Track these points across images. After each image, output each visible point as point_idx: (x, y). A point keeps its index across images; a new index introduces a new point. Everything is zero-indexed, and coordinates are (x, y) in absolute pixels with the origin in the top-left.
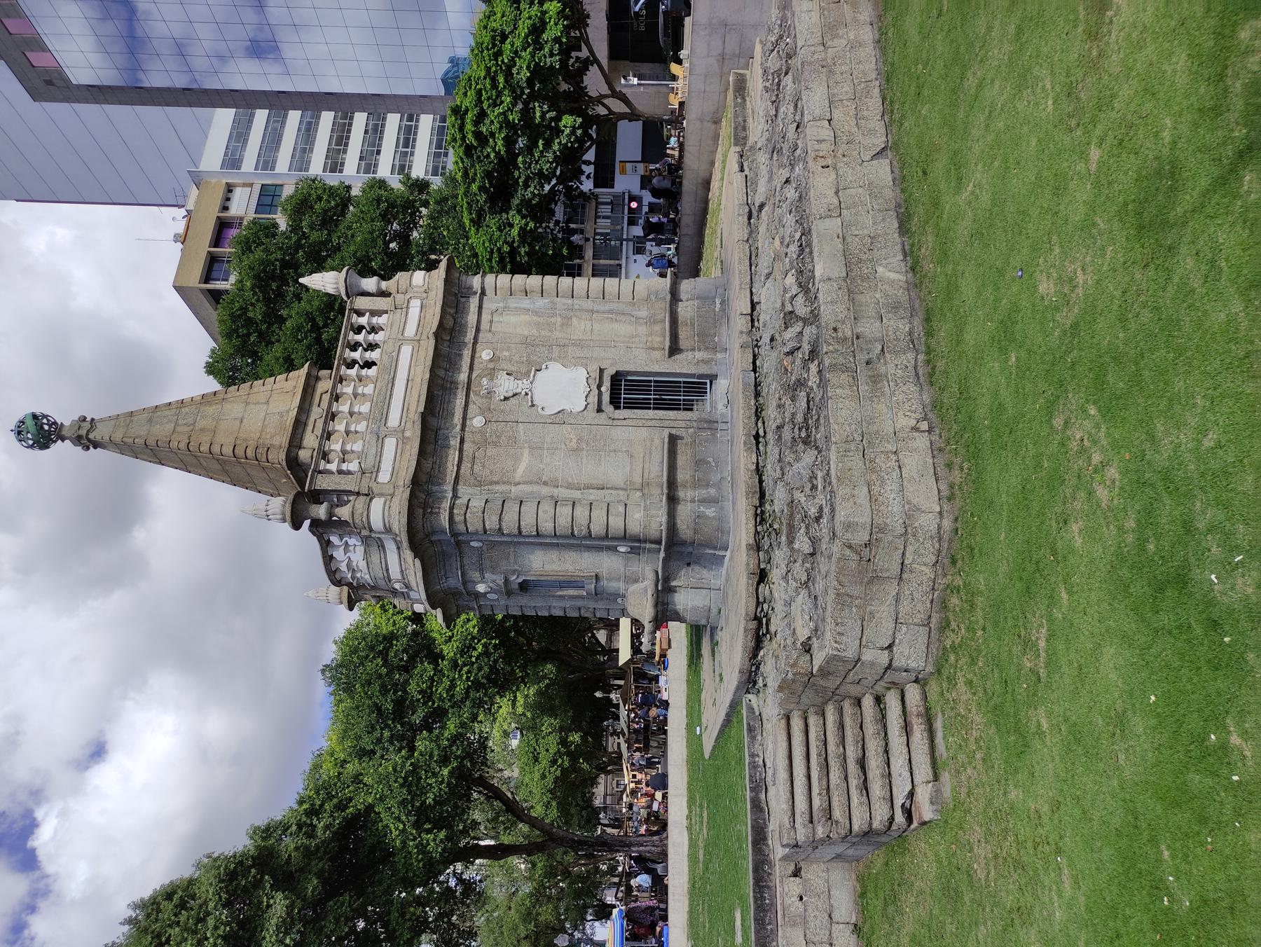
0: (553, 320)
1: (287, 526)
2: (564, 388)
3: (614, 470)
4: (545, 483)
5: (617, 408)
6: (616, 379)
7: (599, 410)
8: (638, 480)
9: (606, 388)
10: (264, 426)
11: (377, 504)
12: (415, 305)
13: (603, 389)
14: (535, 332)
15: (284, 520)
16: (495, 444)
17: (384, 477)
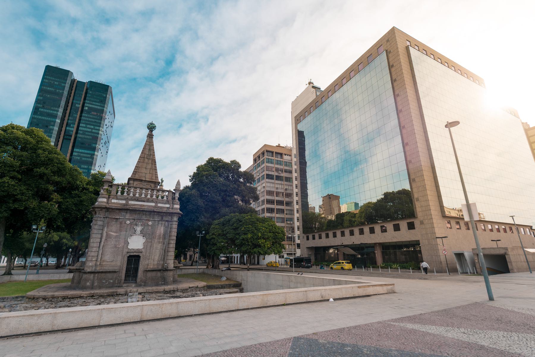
2: (136, 243)
3: (108, 257)
4: (106, 239)
5: (128, 257)
6: (139, 257)
8: (104, 263)
9: (135, 254)
11: (105, 200)
14: (157, 235)
16: (121, 227)
17: (113, 201)
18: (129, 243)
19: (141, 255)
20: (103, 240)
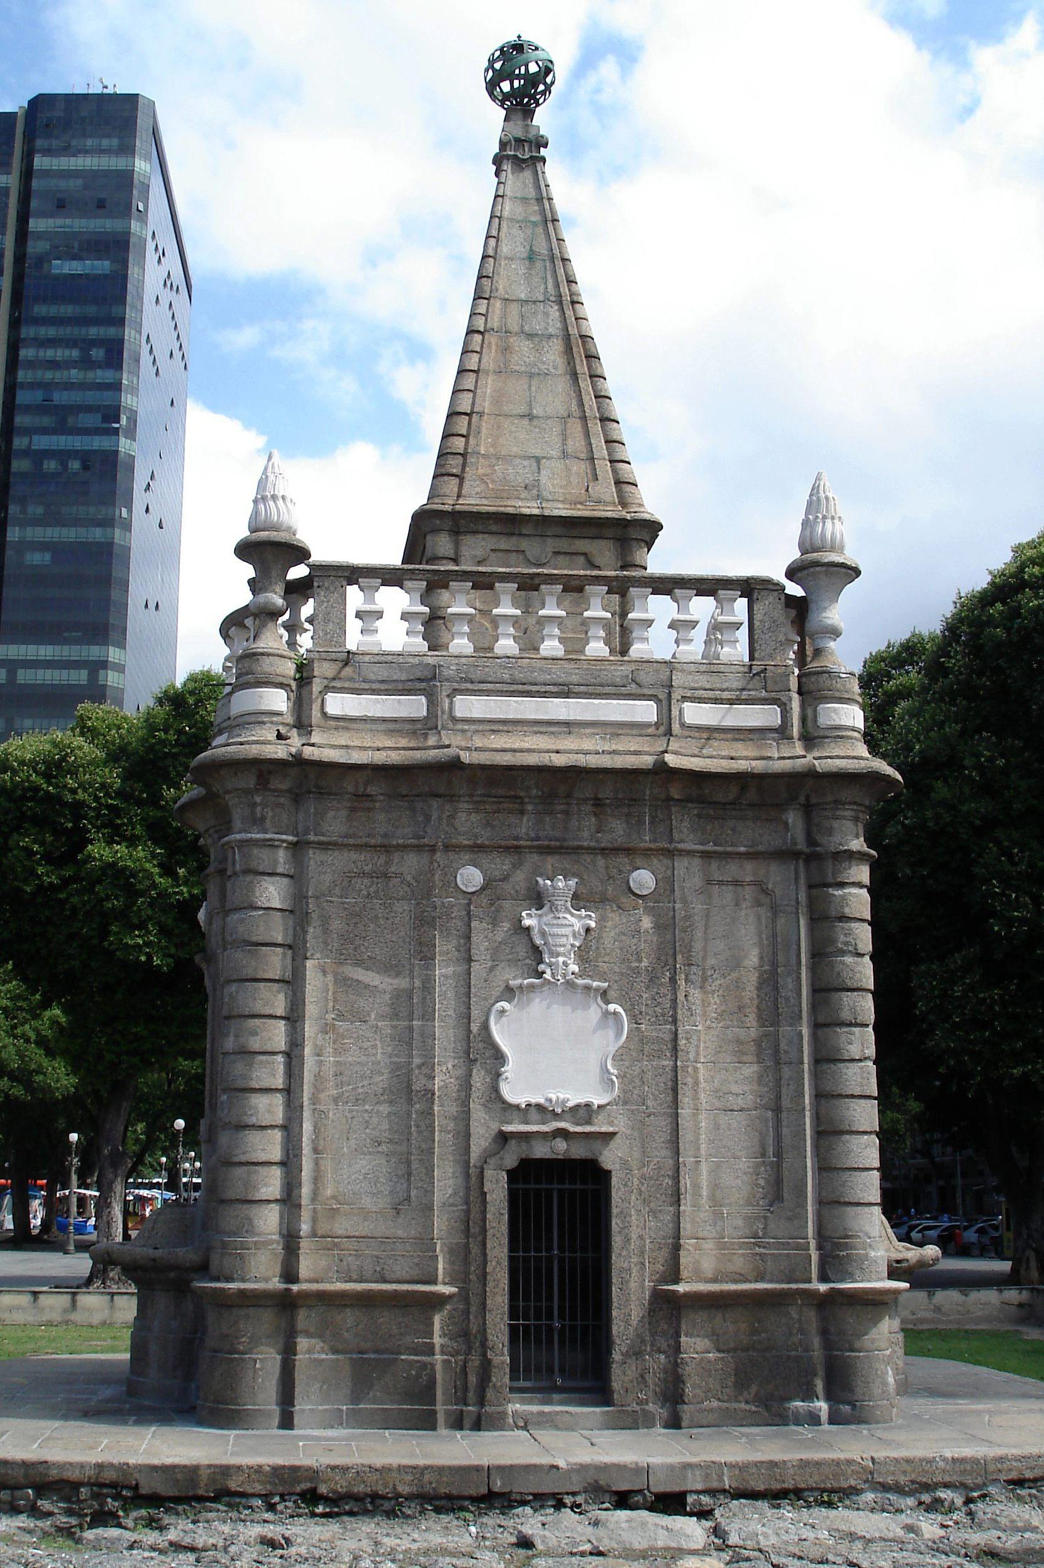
0: (751, 1020)
1: (244, 533)
2: (557, 1058)
5: (513, 1175)
7: (503, 1138)
8: (341, 1226)
10: (507, 459)
12: (764, 716)
13: (561, 1146)
15: (253, 530)
17: (338, 704)
18: (499, 1057)
19: (610, 1158)
20: (310, 1029)
